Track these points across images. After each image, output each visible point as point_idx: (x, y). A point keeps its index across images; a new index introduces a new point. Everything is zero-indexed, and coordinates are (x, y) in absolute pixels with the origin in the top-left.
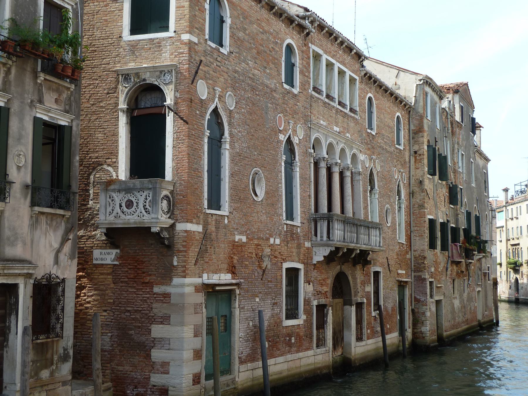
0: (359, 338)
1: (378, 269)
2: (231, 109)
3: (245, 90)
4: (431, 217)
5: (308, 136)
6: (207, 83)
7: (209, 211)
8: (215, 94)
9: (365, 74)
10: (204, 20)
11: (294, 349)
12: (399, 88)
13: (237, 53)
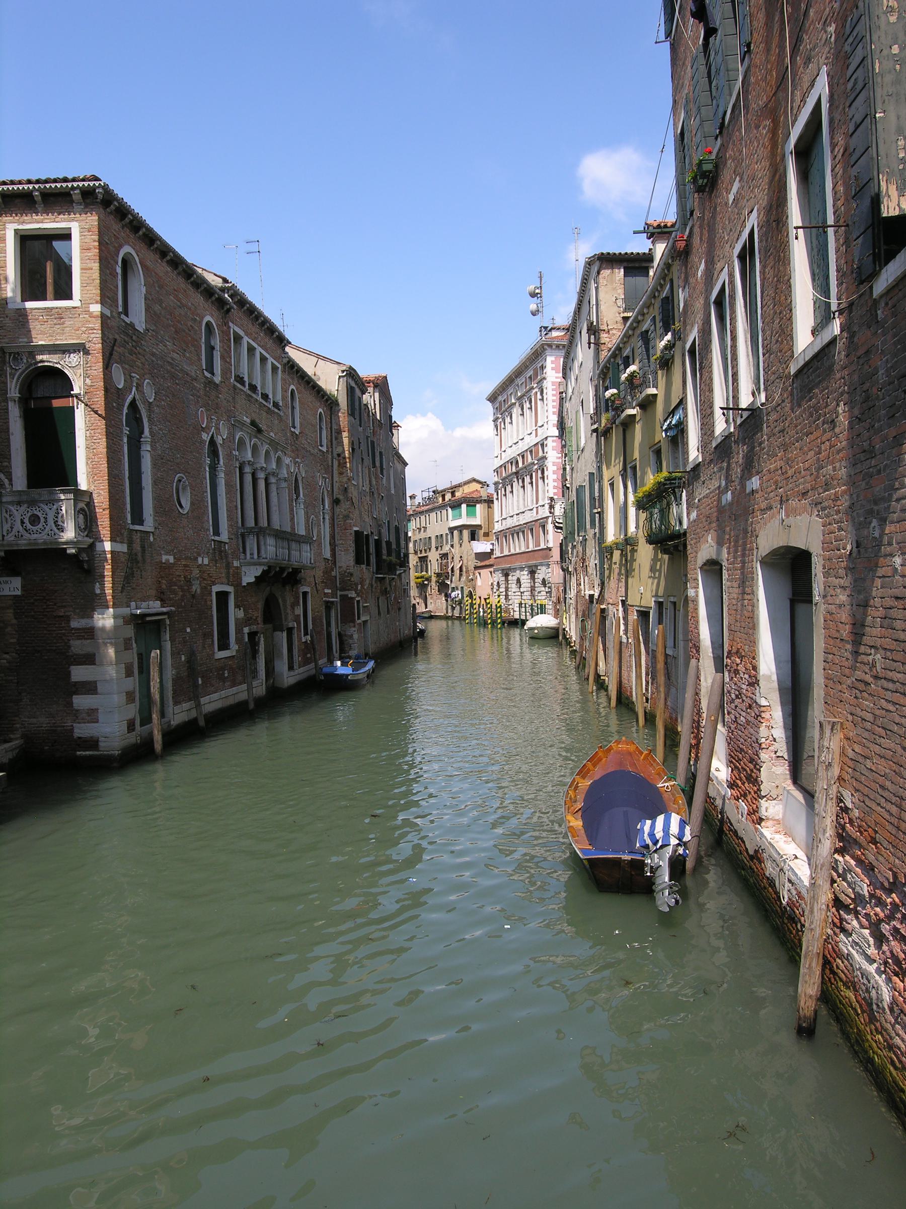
0: (291, 668)
1: (306, 589)
4: (356, 529)
5: (231, 436)
6: (123, 368)
7: (132, 527)
8: (132, 382)
9: (289, 362)
11: (227, 684)
12: (319, 379)
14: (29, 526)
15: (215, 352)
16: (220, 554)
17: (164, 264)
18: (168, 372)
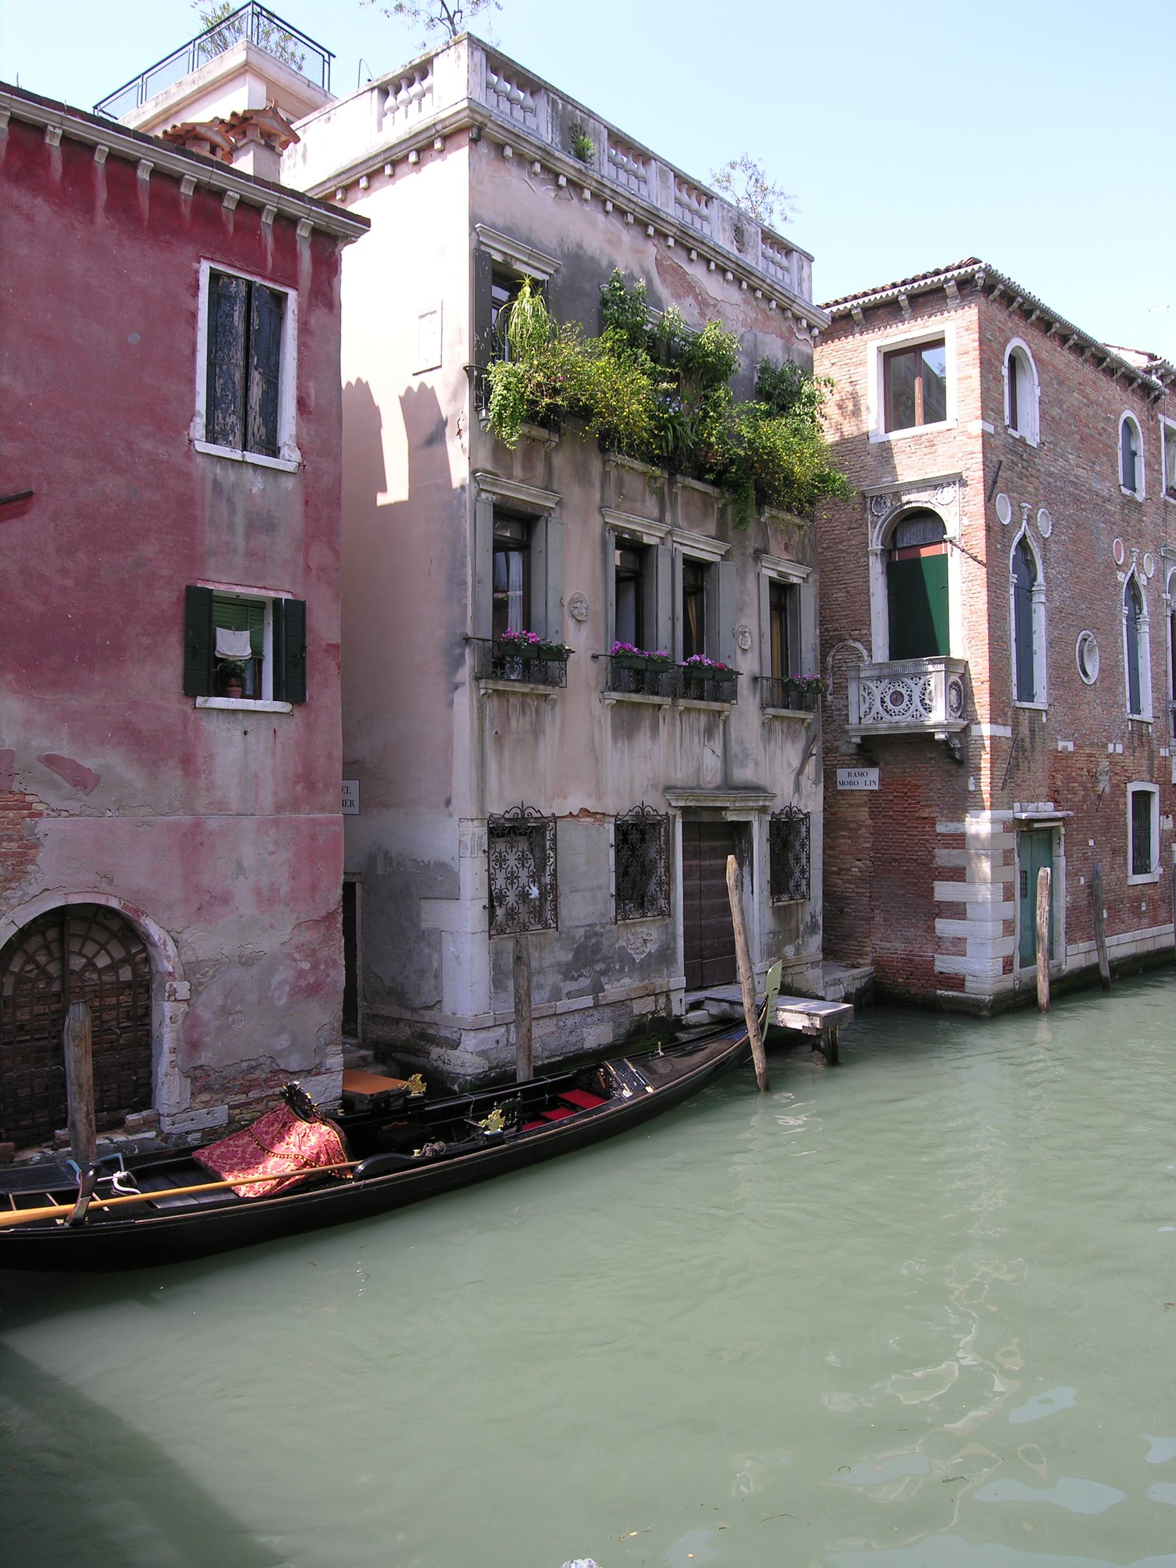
2: (1046, 536)
3: (1064, 503)
5: (1161, 572)
6: (1009, 497)
7: (1018, 704)
8: (1022, 514)
10: (1002, 394)
11: (1145, 921)
13: (1050, 443)
14: (890, 706)
15: (1136, 459)
16: (1140, 739)
17: (1066, 352)
18: (1070, 494)
